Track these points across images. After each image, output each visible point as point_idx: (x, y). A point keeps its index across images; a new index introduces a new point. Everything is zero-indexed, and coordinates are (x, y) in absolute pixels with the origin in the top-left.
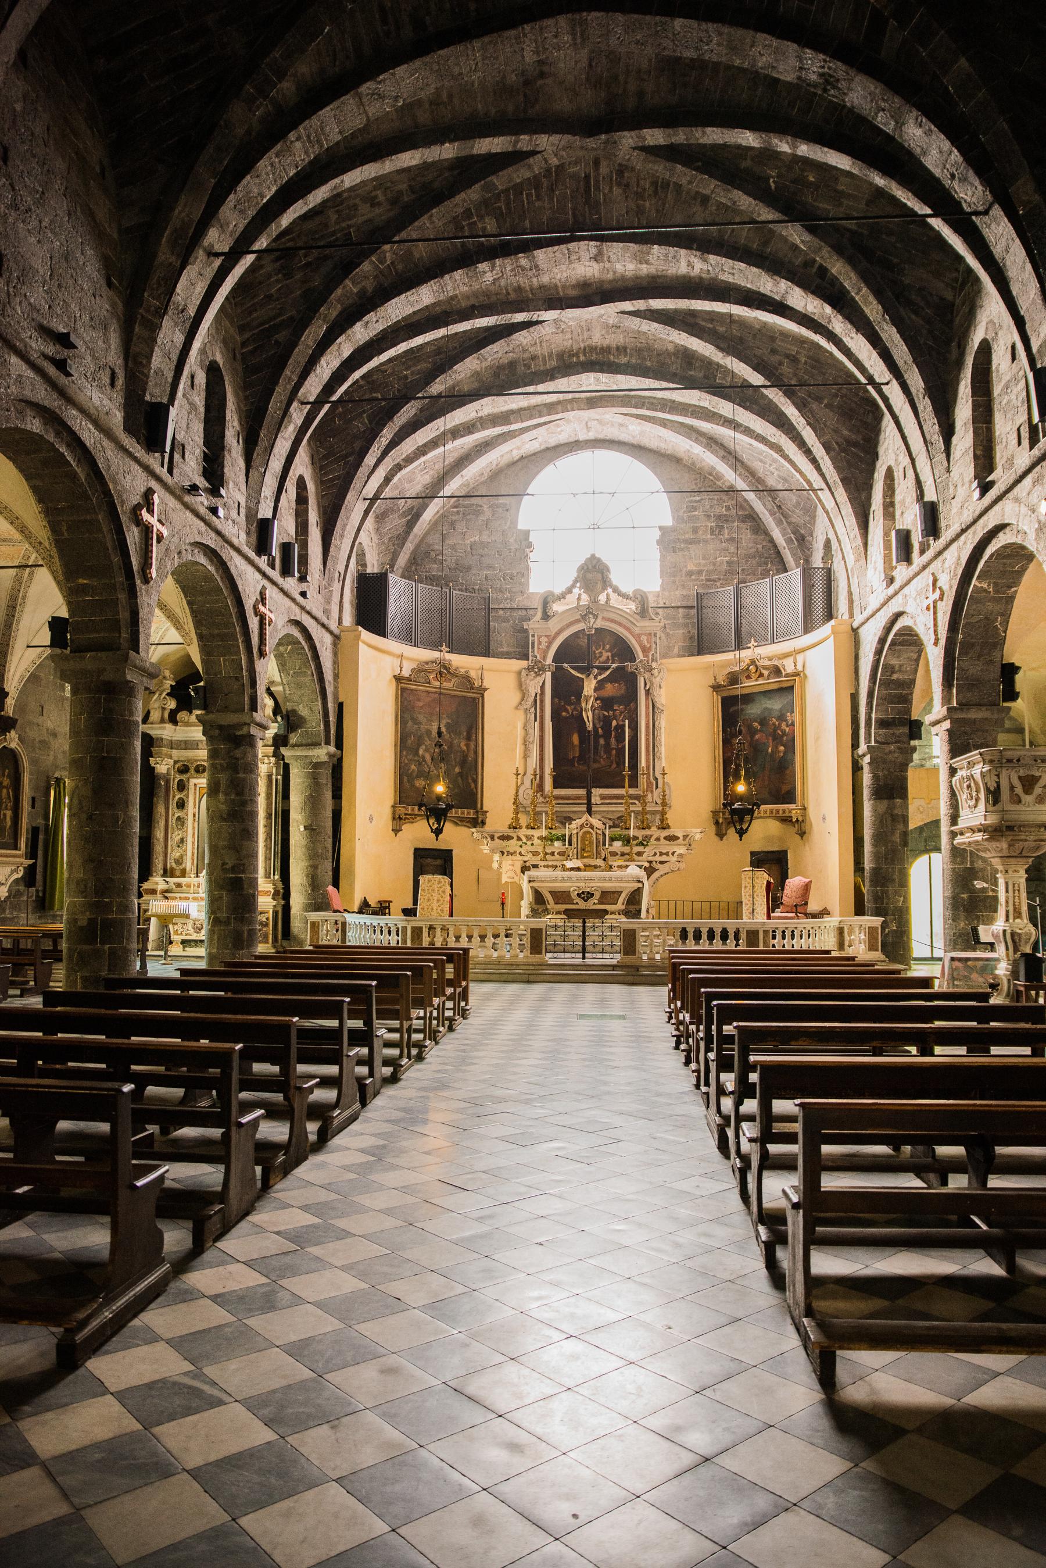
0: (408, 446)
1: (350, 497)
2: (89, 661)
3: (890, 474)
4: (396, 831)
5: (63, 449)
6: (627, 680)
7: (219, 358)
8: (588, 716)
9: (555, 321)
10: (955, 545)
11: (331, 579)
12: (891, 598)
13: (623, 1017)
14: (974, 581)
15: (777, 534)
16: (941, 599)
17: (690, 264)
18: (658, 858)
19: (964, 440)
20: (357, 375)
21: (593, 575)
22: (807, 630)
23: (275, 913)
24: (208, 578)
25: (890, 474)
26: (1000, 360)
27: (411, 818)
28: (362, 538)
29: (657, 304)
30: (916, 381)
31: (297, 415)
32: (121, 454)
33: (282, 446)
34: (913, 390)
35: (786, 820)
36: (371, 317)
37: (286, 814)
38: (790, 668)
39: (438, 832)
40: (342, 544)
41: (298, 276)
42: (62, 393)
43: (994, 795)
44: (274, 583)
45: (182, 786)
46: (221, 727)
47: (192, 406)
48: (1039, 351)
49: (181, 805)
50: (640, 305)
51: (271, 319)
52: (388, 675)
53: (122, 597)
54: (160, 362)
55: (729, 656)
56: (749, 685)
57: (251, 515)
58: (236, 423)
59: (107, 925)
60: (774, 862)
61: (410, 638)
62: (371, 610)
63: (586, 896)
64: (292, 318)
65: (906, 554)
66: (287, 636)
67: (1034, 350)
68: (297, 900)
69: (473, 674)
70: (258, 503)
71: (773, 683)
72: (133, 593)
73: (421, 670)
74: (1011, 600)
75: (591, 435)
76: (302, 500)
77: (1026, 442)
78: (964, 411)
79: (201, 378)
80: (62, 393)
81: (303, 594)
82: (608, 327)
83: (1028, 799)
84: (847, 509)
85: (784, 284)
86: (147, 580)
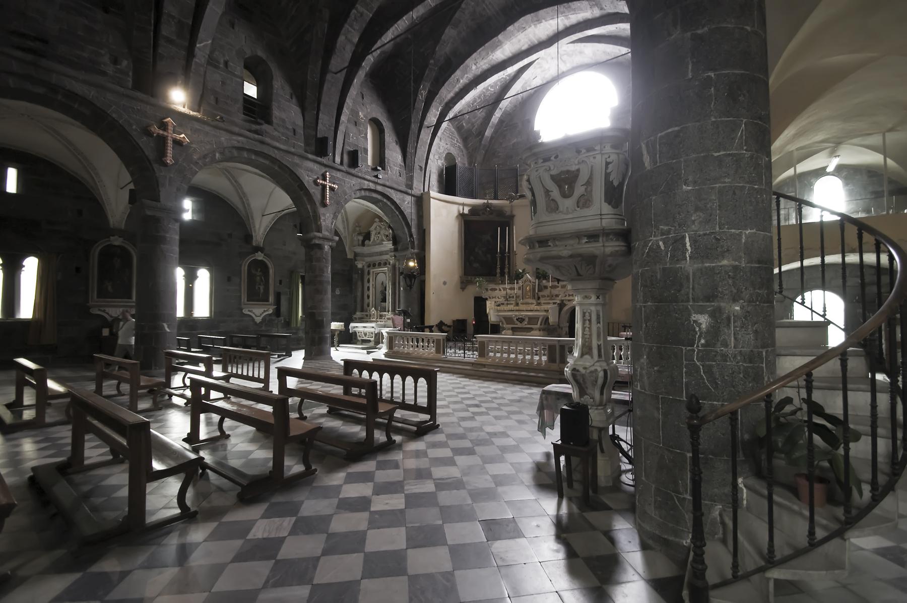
4: (463, 289)
18: (567, 298)
45: (369, 273)
49: (369, 281)
52: (456, 214)
73: (474, 210)
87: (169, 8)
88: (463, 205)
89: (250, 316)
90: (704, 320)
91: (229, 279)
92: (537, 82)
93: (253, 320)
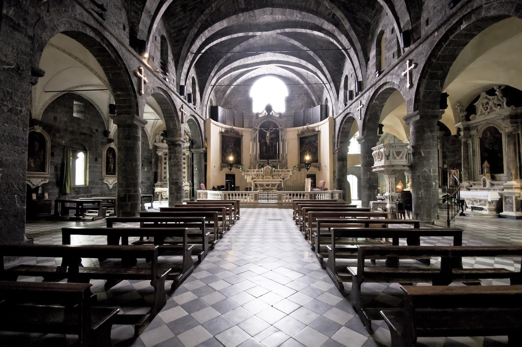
0: (222, 71)
1: (207, 84)
2: (123, 117)
3: (347, 77)
4: (221, 170)
5: (104, 46)
6: (277, 133)
7: (165, 34)
8: (268, 141)
9: (260, 36)
10: (368, 92)
11: (203, 106)
12: (346, 110)
13: (281, 220)
14: (374, 101)
15: (313, 98)
16: (363, 107)
17: (297, 16)
19: (372, 61)
20: (207, 47)
21: (269, 109)
22: (321, 120)
23: (190, 191)
24: (165, 99)
25: (347, 77)
26: (387, 35)
27: (224, 167)
28: (209, 94)
29: (287, 30)
30: (358, 46)
31: (190, 57)
32: (128, 53)
33: (186, 65)
34: (357, 50)
35: (315, 167)
36: (209, 28)
37: (193, 166)
38: (317, 130)
39: (231, 169)
40: (206, 97)
41: (188, 13)
42: (101, 24)
43: (388, 157)
44: (186, 104)
46: (171, 142)
47: (156, 46)
48: (404, 27)
50: (282, 31)
51: (181, 26)
52: (219, 132)
53: (133, 98)
54: (142, 27)
55: (302, 127)
56: (306, 134)
57: (178, 84)
58: (172, 56)
59: (130, 196)
60: (313, 177)
61: (224, 122)
62: (214, 114)
63: (268, 185)
64: (187, 26)
65: (351, 98)
66: (191, 119)
67: (402, 27)
68: (195, 187)
69: (240, 132)
70: (180, 81)
71: (312, 134)
72: (136, 97)
73: (227, 131)
74: (383, 106)
75: (268, 73)
76: (194, 83)
77: (396, 57)
78: (373, 53)
79: (159, 39)
80: (101, 24)
81: (195, 108)
82: (274, 38)
83: (398, 158)
84: (334, 88)
85: (322, 20)
86: (140, 94)
87: (151, 4)
88: (222, 127)
89: (107, 184)
90: (434, 183)
91: (96, 160)
92: (254, 75)
93: (108, 187)
